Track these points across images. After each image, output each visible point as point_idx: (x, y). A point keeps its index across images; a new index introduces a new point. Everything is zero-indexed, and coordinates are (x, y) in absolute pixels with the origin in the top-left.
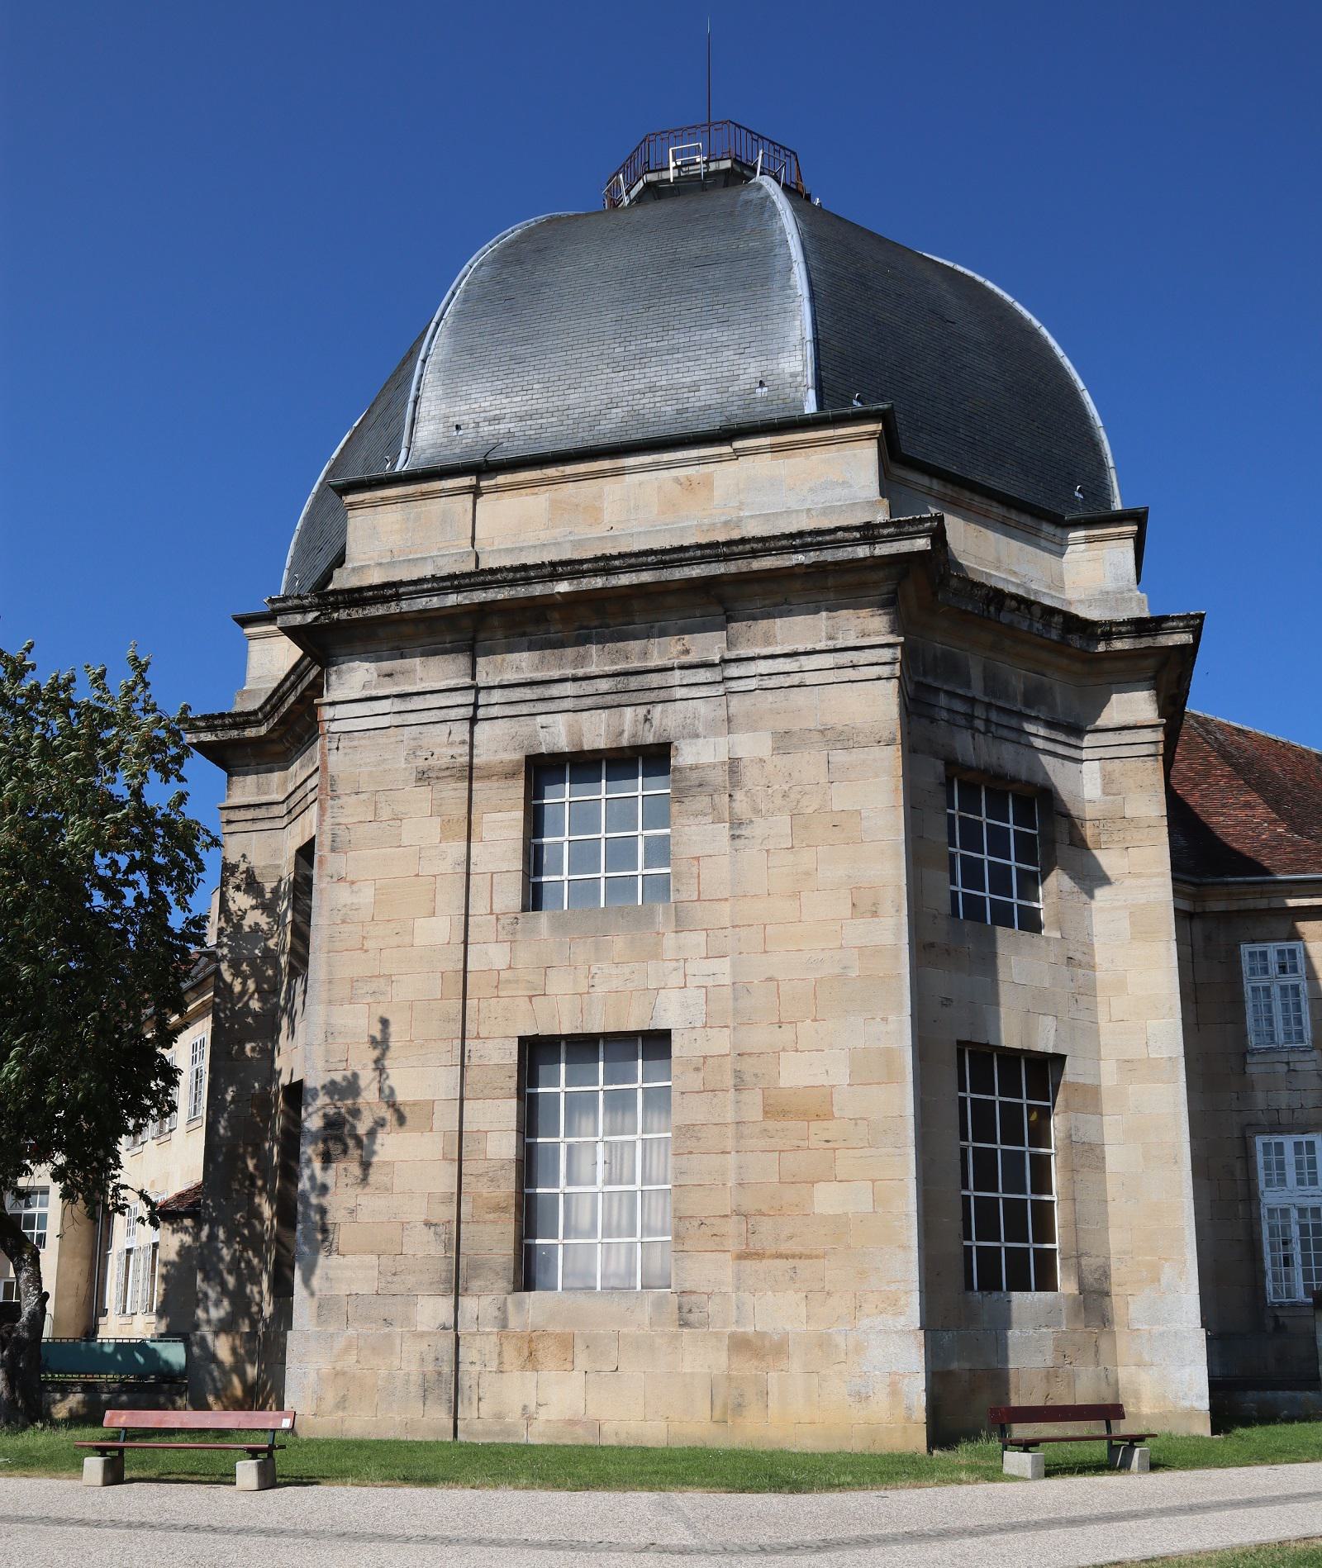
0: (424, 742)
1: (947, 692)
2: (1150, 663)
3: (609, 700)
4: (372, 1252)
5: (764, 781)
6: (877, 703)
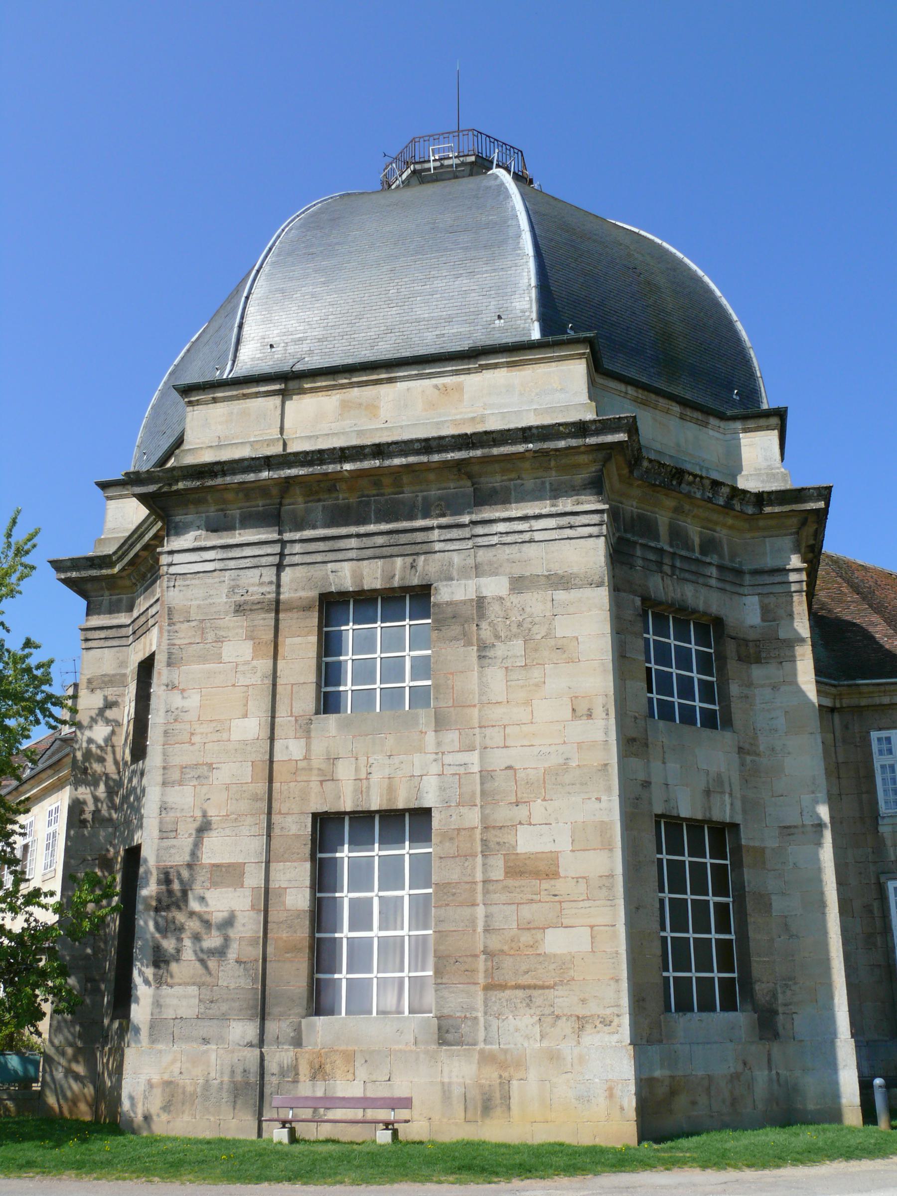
2: (794, 521)
4: (194, 984)
5: (502, 614)
6: (589, 554)
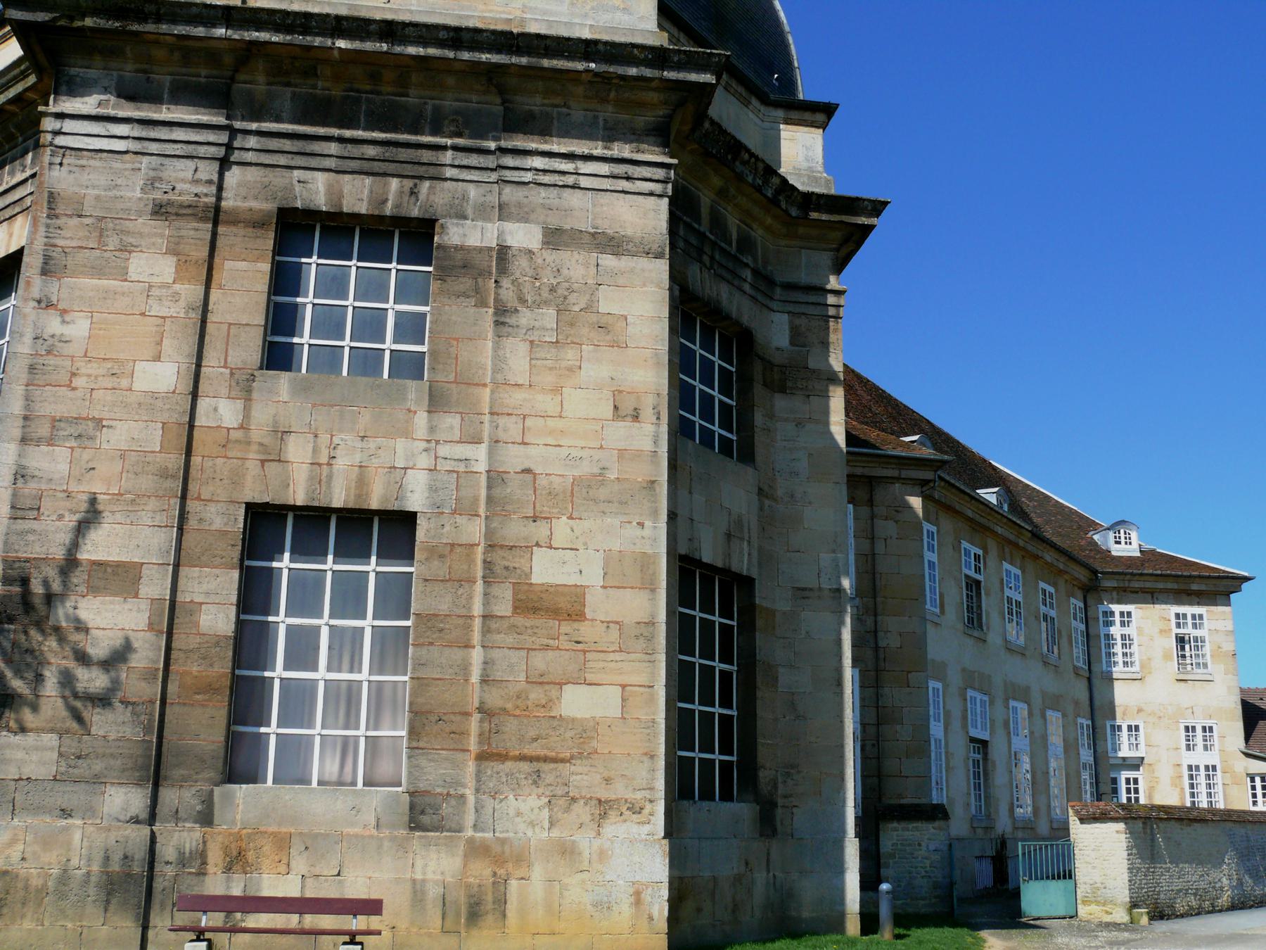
0: (165, 175)
1: (685, 223)
2: (837, 235)
3: (377, 166)
4: (52, 731)
5: (531, 272)
6: (646, 216)
